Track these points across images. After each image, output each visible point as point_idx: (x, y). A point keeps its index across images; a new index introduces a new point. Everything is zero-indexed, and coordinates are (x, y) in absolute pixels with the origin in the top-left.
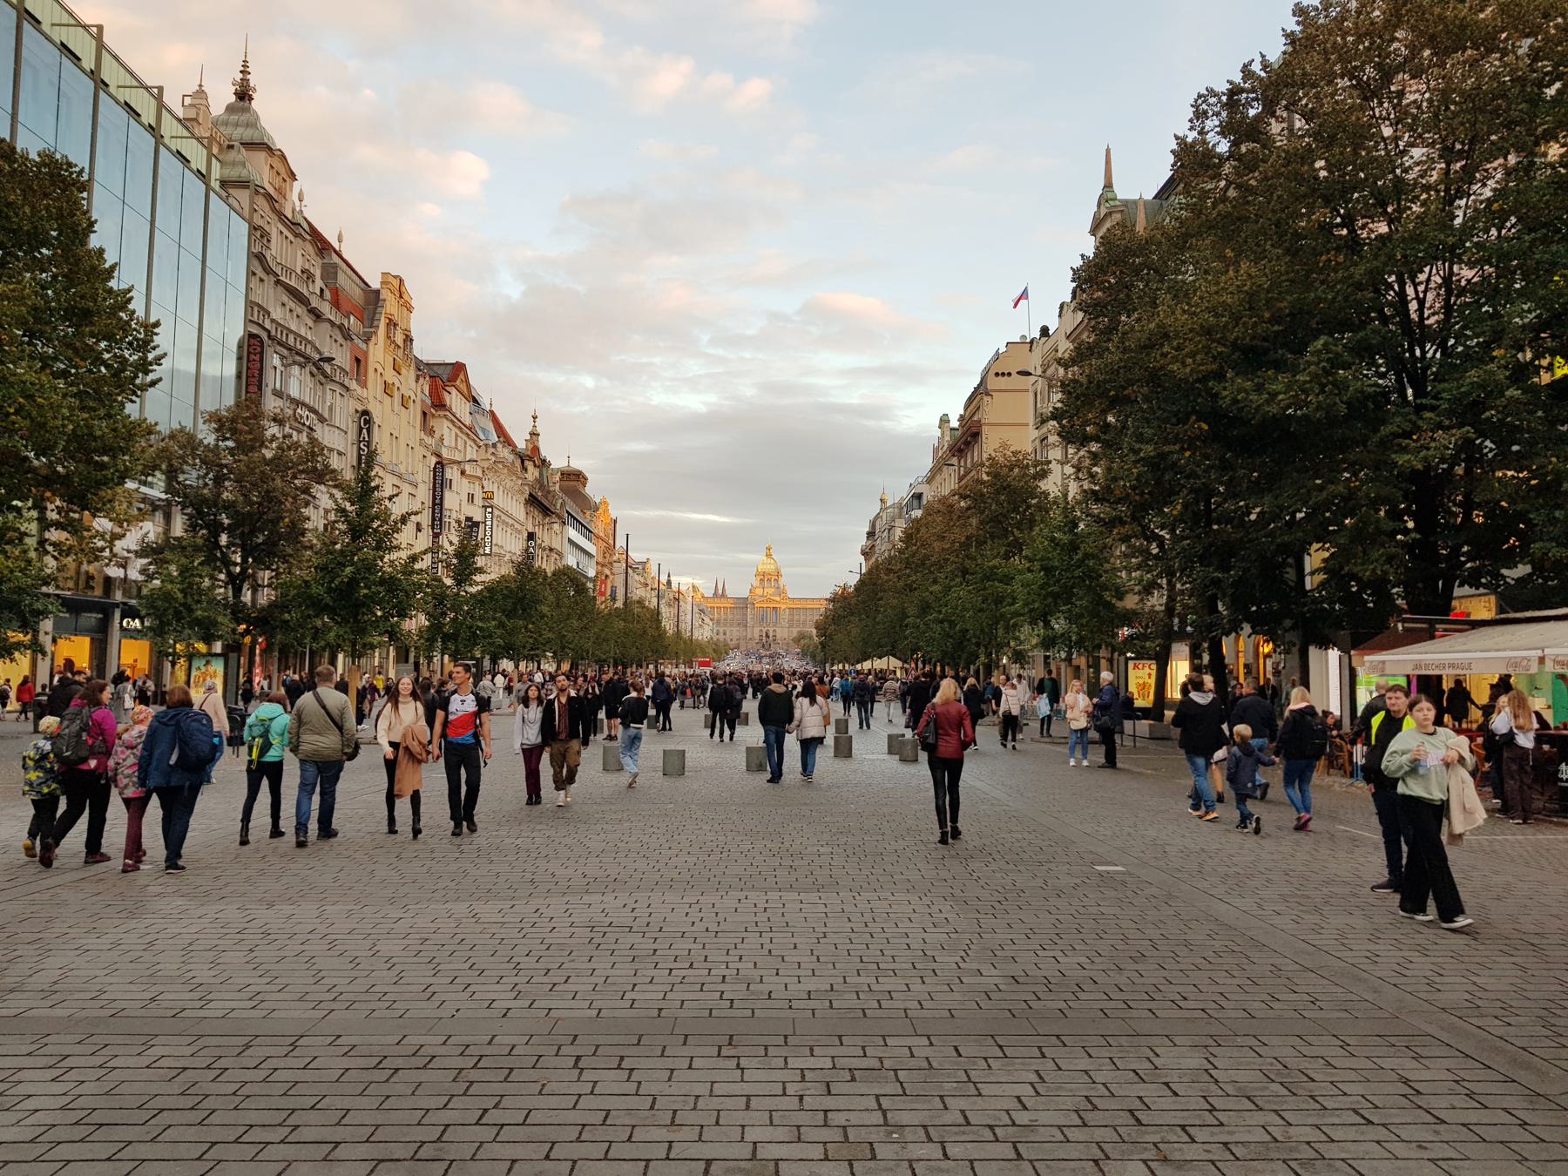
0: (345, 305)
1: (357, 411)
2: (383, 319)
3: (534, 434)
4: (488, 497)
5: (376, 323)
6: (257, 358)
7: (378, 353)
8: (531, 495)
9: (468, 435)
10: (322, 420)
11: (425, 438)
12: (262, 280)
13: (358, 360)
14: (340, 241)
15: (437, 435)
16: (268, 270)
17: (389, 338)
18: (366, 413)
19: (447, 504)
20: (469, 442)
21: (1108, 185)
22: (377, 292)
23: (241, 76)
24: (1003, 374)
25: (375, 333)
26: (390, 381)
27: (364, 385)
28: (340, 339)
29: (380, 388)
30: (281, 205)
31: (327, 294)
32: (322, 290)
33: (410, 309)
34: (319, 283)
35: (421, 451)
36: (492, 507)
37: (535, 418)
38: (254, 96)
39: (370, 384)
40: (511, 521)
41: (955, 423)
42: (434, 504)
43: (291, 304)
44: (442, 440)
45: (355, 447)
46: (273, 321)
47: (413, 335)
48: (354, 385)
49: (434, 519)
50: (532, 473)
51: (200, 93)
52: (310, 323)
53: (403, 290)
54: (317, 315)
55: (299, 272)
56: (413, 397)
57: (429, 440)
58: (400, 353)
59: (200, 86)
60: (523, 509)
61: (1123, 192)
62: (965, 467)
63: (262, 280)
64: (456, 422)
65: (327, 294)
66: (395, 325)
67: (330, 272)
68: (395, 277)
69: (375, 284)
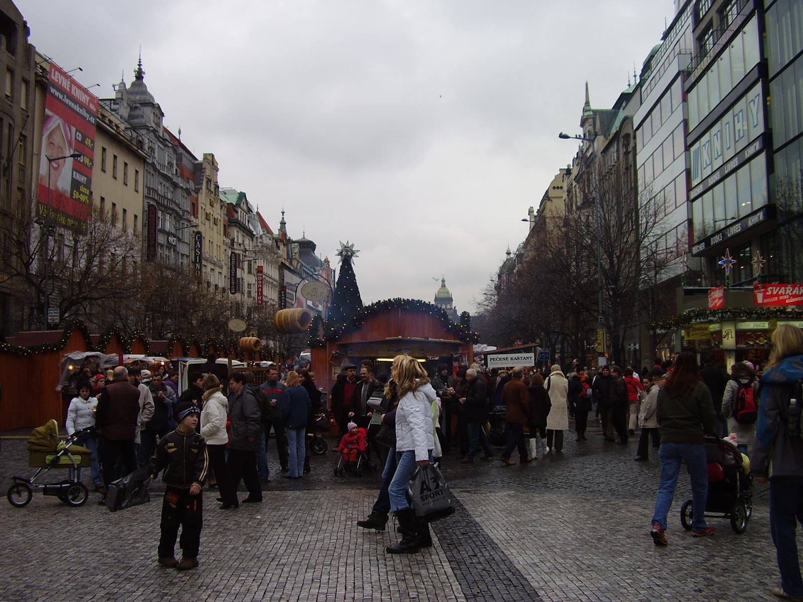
1: (194, 232)
2: (204, 179)
3: (283, 224)
5: (201, 182)
6: (154, 216)
7: (203, 198)
10: (179, 240)
11: (225, 239)
12: (153, 175)
13: (193, 204)
14: (180, 134)
17: (207, 188)
18: (199, 233)
21: (587, 103)
22: (201, 164)
23: (138, 67)
24: (558, 188)
25: (201, 188)
27: (197, 218)
28: (186, 195)
29: (204, 217)
33: (217, 170)
35: (223, 247)
37: (283, 213)
38: (144, 76)
39: (199, 216)
40: (271, 281)
48: (192, 218)
50: (282, 251)
51: (123, 84)
52: (172, 190)
54: (175, 185)
55: (166, 165)
58: (213, 195)
59: (123, 80)
60: (278, 272)
61: (594, 106)
63: (153, 175)
66: (211, 181)
68: (209, 154)
69: (200, 158)
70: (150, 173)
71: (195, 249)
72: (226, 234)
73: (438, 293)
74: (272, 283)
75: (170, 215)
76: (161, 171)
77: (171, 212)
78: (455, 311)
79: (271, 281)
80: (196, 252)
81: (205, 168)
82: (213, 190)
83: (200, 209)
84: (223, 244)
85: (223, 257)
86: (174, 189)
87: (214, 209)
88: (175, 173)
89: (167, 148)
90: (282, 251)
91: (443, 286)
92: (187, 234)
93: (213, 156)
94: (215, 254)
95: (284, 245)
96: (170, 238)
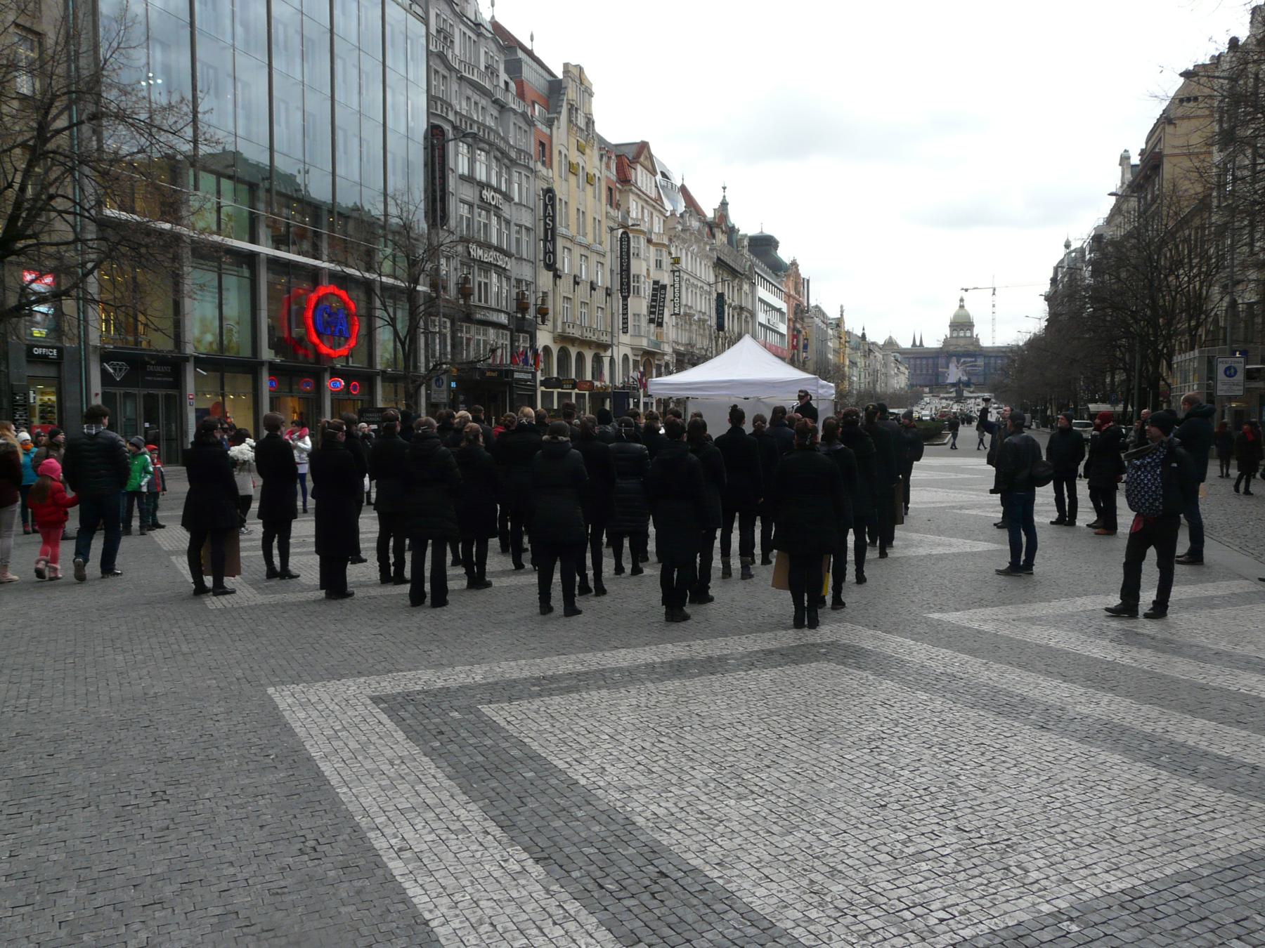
0: (529, 96)
2: (565, 104)
3: (724, 204)
4: (677, 261)
5: (559, 109)
7: (561, 136)
8: (719, 259)
9: (654, 207)
13: (542, 144)
15: (623, 207)
16: (450, 68)
17: (570, 121)
19: (633, 271)
20: (655, 214)
25: (558, 119)
26: (574, 161)
28: (525, 127)
30: (463, 8)
31: (512, 85)
32: (506, 83)
33: (591, 95)
34: (503, 76)
36: (679, 271)
37: (724, 188)
40: (700, 284)
41: (1135, 160)
42: (622, 270)
43: (475, 97)
44: (628, 212)
45: (542, 222)
46: (456, 113)
47: (596, 117)
48: (539, 166)
49: (622, 284)
52: (495, 113)
53: (583, 77)
54: (502, 107)
56: (598, 174)
57: (614, 213)
60: (711, 272)
62: (1146, 203)
64: (642, 196)
65: (512, 85)
66: (577, 109)
67: (514, 68)
68: (576, 66)
70: (520, 128)
71: (545, 217)
72: (611, 201)
73: (955, 316)
74: (702, 287)
75: (487, 153)
76: (466, 75)
77: (487, 147)
78: (977, 340)
79: (700, 284)
80: (546, 224)
81: (566, 88)
82: (583, 125)
83: (555, 153)
84: (607, 217)
85: (606, 238)
86: (500, 112)
87: (586, 158)
88: (502, 85)
89: (482, 39)
90: (721, 238)
91: (962, 307)
92: (522, 188)
93: (581, 69)
94: (589, 229)
95: (723, 232)
96: (484, 192)
